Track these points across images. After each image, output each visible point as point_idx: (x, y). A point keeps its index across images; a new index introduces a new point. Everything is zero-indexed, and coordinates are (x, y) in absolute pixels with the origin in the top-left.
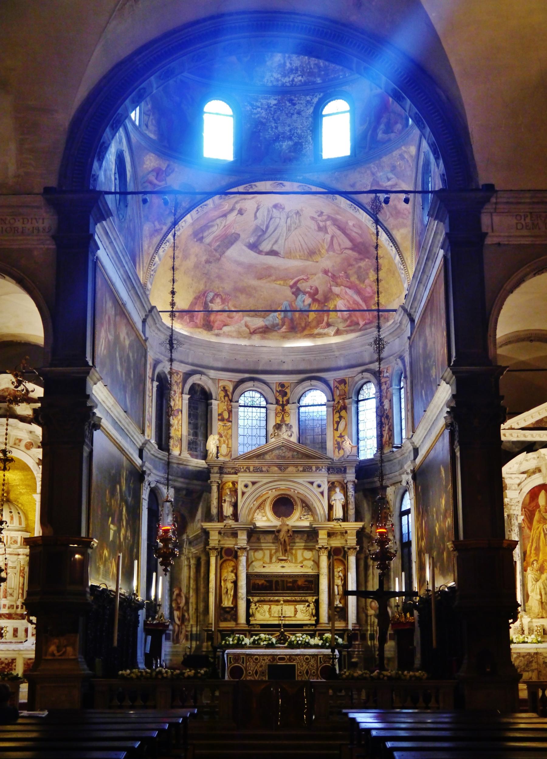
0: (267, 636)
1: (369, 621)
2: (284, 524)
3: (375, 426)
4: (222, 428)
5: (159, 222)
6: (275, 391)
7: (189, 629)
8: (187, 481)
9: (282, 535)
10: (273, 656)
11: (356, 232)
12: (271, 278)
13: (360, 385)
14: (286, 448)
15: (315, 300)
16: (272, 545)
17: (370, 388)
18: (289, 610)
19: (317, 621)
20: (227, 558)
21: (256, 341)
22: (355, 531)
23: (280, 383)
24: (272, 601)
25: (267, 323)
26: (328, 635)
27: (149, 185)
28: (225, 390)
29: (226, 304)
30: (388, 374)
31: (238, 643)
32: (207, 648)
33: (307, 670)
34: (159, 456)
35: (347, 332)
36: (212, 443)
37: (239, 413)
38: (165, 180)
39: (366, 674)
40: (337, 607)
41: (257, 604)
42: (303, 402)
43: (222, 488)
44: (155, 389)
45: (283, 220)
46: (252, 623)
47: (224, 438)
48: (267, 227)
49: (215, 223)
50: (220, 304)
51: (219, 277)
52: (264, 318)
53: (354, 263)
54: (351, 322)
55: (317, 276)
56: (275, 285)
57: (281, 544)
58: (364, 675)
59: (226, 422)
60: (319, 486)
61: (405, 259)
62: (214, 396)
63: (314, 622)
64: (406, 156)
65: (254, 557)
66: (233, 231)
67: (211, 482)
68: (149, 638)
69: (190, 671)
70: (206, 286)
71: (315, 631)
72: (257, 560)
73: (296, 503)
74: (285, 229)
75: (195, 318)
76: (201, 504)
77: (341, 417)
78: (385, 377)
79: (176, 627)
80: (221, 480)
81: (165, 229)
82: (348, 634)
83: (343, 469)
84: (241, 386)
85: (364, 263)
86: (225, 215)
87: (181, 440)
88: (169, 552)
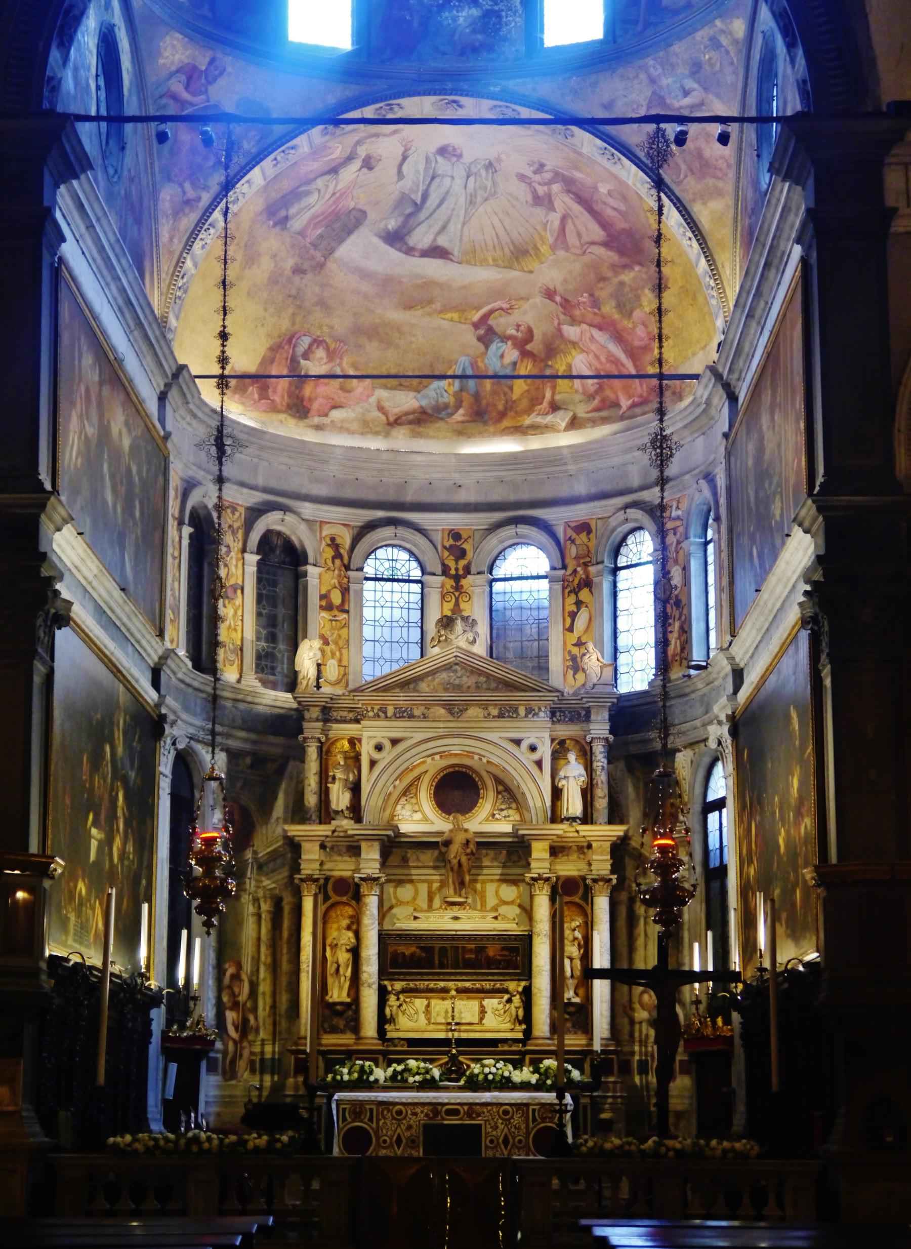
0: (422, 1065)
1: (637, 1034)
2: (458, 829)
3: (652, 622)
4: (328, 626)
5: (193, 184)
6: (440, 548)
7: (257, 1049)
8: (253, 736)
9: (455, 848)
10: (435, 1107)
12: (434, 306)
13: (621, 535)
14: (463, 668)
15: (525, 354)
16: (433, 872)
17: (642, 543)
18: (467, 1009)
19: (528, 1033)
20: (338, 899)
21: (401, 440)
22: (609, 844)
23: (451, 530)
25: (424, 403)
26: (550, 1063)
27: (171, 102)
28: (334, 544)
29: (338, 361)
30: (679, 513)
31: (360, 1078)
32: (296, 1088)
33: (506, 1136)
34: (196, 684)
35: (594, 422)
36: (307, 657)
37: (365, 593)
38: (206, 91)
39: (630, 1144)
40: (570, 1004)
41: (402, 997)
42: (501, 570)
43: (328, 752)
44: (186, 542)
46: (389, 1035)
47: (332, 646)
48: (425, 196)
49: (312, 187)
50: (325, 360)
51: (323, 304)
52: (419, 392)
53: (609, 274)
54: (603, 401)
57: (452, 869)
58: (627, 1147)
59: (336, 612)
60: (533, 749)
61: (720, 267)
63: (520, 1036)
64: (724, 41)
65: (396, 897)
67: (305, 739)
68: (173, 1067)
69: (260, 1137)
70: (293, 323)
71: (523, 1054)
72: (400, 903)
73: (484, 783)
74: (462, 200)
75: (270, 391)
76: (283, 786)
77: (579, 604)
79: (231, 1046)
80: (327, 736)
81: (206, 198)
82: (592, 1060)
83: (583, 713)
84: (368, 536)
85: (632, 274)
86: (334, 170)
87: (241, 649)
88: (216, 886)
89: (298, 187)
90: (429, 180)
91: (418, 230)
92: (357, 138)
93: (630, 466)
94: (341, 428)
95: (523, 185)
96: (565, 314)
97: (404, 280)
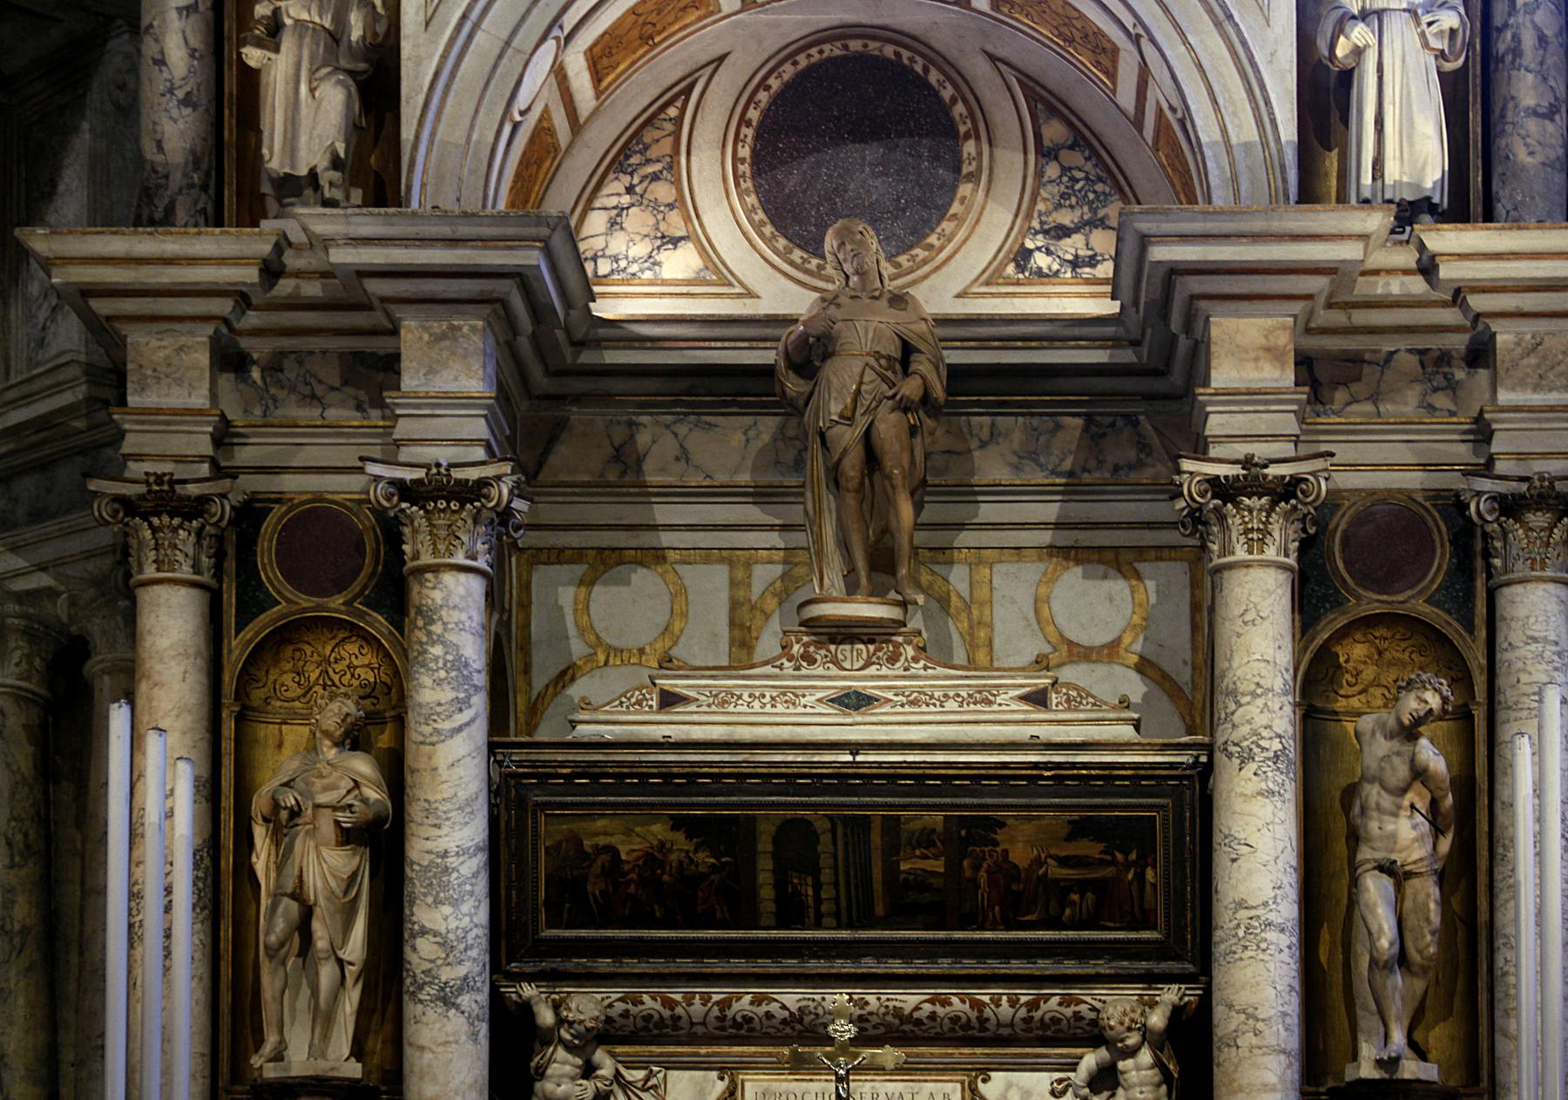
9: (844, 379)
24: (742, 1031)
41: (600, 1055)
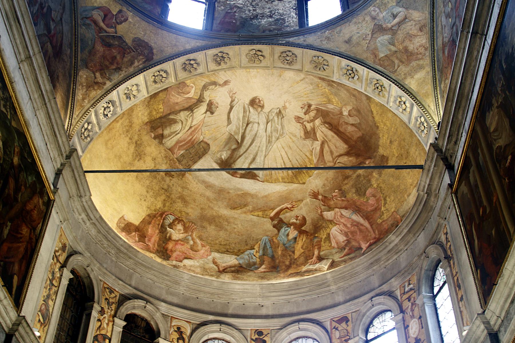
5: (101, 75)
6: (249, 339)
11: (352, 125)
12: (248, 208)
15: (301, 232)
21: (226, 278)
25: (241, 262)
27: (93, 25)
28: (179, 330)
38: (115, 27)
44: (65, 282)
45: (262, 126)
48: (243, 138)
49: (177, 117)
50: (182, 232)
51: (182, 198)
52: (238, 256)
55: (304, 202)
56: (252, 217)
61: (427, 107)
62: (162, 333)
66: (201, 138)
70: (164, 206)
74: (264, 140)
78: (408, 292)
81: (109, 85)
86: (190, 109)
89: (169, 114)
90: (245, 125)
91: (239, 160)
92: (203, 83)
93: (372, 277)
94: (190, 270)
95: (299, 124)
96: (324, 206)
97: (231, 191)
